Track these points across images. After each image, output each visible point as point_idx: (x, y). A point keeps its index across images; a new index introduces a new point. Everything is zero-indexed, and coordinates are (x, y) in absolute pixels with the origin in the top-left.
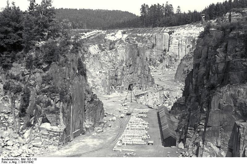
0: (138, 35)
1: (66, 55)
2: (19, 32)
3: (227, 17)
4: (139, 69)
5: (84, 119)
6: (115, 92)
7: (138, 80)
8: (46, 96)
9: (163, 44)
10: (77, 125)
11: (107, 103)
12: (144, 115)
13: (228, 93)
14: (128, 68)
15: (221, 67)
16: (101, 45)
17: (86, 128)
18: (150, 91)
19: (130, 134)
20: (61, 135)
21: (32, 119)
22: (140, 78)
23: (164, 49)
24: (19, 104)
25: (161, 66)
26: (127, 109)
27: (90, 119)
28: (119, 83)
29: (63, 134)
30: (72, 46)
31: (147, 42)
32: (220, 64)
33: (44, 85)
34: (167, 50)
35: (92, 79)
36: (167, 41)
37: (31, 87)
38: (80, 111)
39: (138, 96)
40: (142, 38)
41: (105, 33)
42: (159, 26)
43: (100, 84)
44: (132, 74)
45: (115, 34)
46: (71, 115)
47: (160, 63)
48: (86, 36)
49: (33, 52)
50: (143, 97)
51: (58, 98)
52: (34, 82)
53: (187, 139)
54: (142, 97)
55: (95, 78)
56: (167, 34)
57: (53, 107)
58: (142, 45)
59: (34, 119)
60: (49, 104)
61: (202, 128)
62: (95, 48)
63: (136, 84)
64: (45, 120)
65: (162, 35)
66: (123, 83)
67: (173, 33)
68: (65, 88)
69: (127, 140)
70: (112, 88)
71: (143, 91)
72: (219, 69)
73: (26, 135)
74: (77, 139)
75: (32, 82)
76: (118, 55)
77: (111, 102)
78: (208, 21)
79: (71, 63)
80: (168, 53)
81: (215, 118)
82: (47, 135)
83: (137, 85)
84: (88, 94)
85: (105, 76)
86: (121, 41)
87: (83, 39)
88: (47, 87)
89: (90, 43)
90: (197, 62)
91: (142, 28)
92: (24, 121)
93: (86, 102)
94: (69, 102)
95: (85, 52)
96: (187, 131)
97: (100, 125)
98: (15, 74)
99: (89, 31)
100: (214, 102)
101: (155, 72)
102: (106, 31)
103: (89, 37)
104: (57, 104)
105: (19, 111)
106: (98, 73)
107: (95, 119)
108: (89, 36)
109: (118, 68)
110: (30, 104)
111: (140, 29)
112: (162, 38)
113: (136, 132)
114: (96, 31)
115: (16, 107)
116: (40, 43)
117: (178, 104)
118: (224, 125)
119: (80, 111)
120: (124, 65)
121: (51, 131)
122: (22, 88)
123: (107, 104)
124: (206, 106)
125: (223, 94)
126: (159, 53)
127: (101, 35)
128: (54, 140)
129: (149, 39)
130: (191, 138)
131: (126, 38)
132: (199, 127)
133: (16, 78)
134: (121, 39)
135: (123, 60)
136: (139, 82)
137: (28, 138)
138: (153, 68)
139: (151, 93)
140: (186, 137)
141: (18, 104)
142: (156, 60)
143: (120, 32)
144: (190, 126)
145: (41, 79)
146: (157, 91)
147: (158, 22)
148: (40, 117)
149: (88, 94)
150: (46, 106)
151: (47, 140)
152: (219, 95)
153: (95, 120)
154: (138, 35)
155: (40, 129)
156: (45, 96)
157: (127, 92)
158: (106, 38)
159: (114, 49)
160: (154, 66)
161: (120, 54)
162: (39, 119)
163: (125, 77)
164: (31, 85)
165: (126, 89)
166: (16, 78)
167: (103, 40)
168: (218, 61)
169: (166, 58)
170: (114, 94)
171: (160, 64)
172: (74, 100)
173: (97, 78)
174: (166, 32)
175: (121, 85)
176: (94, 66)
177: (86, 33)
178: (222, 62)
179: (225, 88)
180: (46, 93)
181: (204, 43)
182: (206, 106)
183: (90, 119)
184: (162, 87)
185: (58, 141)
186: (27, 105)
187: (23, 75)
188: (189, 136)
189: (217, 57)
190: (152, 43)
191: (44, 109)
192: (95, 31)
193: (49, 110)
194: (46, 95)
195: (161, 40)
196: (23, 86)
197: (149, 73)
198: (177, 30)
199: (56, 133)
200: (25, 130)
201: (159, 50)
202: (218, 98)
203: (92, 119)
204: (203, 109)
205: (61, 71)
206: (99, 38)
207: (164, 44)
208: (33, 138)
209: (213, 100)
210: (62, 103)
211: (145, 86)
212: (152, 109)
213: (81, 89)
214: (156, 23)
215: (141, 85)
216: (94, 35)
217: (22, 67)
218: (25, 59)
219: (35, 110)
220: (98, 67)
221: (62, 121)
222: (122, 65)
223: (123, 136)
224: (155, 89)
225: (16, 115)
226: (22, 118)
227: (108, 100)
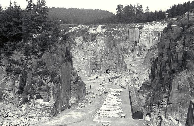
0: (115, 29)
1: (56, 45)
2: (20, 26)
4: (114, 56)
5: (70, 96)
7: (114, 65)
8: (40, 77)
10: (65, 101)
12: (118, 93)
14: (106, 56)
15: (180, 56)
16: (85, 37)
17: (72, 104)
19: (106, 109)
20: (52, 109)
22: (115, 64)
23: (135, 41)
24: (18, 84)
25: (132, 54)
26: (104, 88)
28: (98, 68)
29: (53, 108)
30: (61, 37)
31: (121, 35)
33: (38, 69)
35: (77, 64)
36: (138, 35)
38: (67, 90)
39: (113, 79)
40: (118, 32)
41: (88, 28)
43: (83, 69)
44: (109, 61)
45: (96, 28)
50: (118, 79)
51: (49, 79)
52: (30, 66)
53: (152, 113)
54: (116, 79)
55: (80, 63)
56: (138, 29)
57: (45, 86)
59: (30, 95)
60: (42, 83)
61: (164, 104)
62: (80, 39)
63: (112, 68)
64: (39, 97)
66: (102, 67)
68: (55, 71)
69: (103, 114)
70: (93, 71)
73: (23, 108)
74: (64, 112)
75: (29, 66)
76: (98, 46)
77: (92, 82)
78: (171, 19)
79: (61, 51)
81: (175, 97)
82: (40, 109)
84: (74, 76)
85: (88, 62)
86: (101, 34)
88: (41, 70)
90: (161, 52)
92: (22, 97)
93: (72, 82)
94: (58, 82)
95: (72, 42)
96: (152, 107)
97: (83, 101)
98: (16, 60)
99: (75, 26)
100: (174, 84)
101: (127, 59)
102: (89, 26)
103: (75, 31)
105: (18, 89)
106: (82, 59)
107: (79, 96)
109: (97, 56)
110: (27, 84)
111: (116, 24)
112: (134, 32)
113: (111, 107)
114: (81, 26)
115: (16, 86)
116: (36, 35)
117: (145, 85)
118: (181, 103)
119: (67, 90)
120: (103, 53)
121: (43, 105)
122: (21, 71)
124: (168, 87)
125: (181, 78)
126: (131, 44)
127: (85, 29)
128: (46, 113)
129: (123, 32)
130: (155, 113)
132: (162, 104)
133: (16, 63)
134: (101, 32)
136: (114, 67)
137: (25, 111)
138: (126, 56)
139: (124, 76)
140: (151, 112)
141: (17, 84)
143: (100, 27)
144: (155, 103)
145: (36, 63)
146: (129, 75)
147: (131, 19)
148: (35, 94)
149: (74, 76)
150: (40, 86)
151: (40, 113)
152: (178, 78)
153: (79, 97)
154: (115, 29)
155: (35, 104)
156: (39, 77)
157: (105, 75)
158: (88, 31)
159: (95, 41)
160: (127, 55)
161: (100, 45)
162: (34, 95)
163: (103, 63)
164: (28, 68)
165: (104, 72)
166: (16, 63)
168: (177, 51)
169: (137, 48)
172: (63, 81)
173: (81, 64)
174: (137, 27)
175: (100, 69)
176: (79, 54)
177: (73, 27)
178: (181, 52)
181: (167, 36)
182: (168, 87)
183: (75, 96)
185: (49, 114)
186: (25, 84)
187: (22, 60)
188: (154, 111)
190: (125, 36)
191: (38, 88)
192: (80, 26)
193: (42, 89)
194: (40, 76)
195: (132, 33)
196: (22, 69)
197: (123, 60)
198: (146, 26)
199: (47, 107)
200: (23, 104)
201: (131, 42)
202: (177, 81)
203: (77, 96)
204: (165, 89)
205: (52, 57)
207: (135, 37)
208: (29, 111)
210: (52, 83)
211: (119, 70)
212: (124, 89)
213: (68, 72)
214: (129, 20)
215: (117, 69)
217: (21, 54)
218: (23, 48)
219: (31, 89)
221: (53, 97)
222: (101, 53)
223: (101, 110)
224: (127, 73)
225: (16, 92)
226: (21, 95)
227: (89, 81)
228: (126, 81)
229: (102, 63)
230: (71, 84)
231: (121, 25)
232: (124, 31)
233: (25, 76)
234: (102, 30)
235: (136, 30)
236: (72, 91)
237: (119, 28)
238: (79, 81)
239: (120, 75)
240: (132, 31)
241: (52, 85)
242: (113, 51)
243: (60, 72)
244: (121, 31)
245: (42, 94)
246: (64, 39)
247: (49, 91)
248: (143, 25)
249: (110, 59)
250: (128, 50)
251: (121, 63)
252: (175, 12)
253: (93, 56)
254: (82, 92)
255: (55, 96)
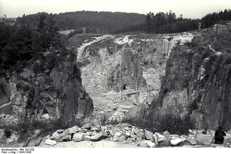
0: (142, 40)
1: (64, 63)
2: (29, 45)
3: (215, 28)
6: (111, 91)
8: (47, 93)
9: (163, 49)
11: (102, 100)
13: (173, 96)
14: (123, 71)
16: (110, 49)
18: (141, 90)
21: (36, 110)
22: (133, 79)
23: (163, 53)
24: (26, 99)
25: (160, 68)
26: (115, 105)
27: (81, 112)
28: (115, 84)
30: (69, 55)
31: (148, 47)
32: (172, 74)
33: (46, 85)
34: (166, 55)
35: (94, 79)
37: (36, 86)
38: (73, 106)
39: (129, 95)
40: (145, 43)
41: (113, 38)
42: (161, 33)
43: (100, 84)
44: (127, 76)
45: (123, 39)
46: (65, 110)
47: (159, 66)
48: (97, 40)
49: (39, 60)
51: (56, 95)
52: (38, 83)
54: (133, 96)
55: (97, 78)
56: (167, 40)
57: (52, 102)
58: (136, 52)
60: (49, 99)
63: (129, 84)
64: (45, 112)
65: (162, 41)
66: (118, 83)
67: (172, 39)
68: (62, 88)
70: (109, 87)
71: (135, 90)
72: (171, 78)
75: (37, 83)
77: (105, 99)
78: (203, 30)
80: (166, 57)
83: (130, 85)
84: (81, 92)
85: (105, 77)
87: (95, 42)
88: (48, 87)
89: (100, 47)
91: (146, 34)
92: (30, 111)
93: (79, 99)
95: (95, 54)
97: (89, 117)
98: (25, 77)
99: (100, 36)
100: (164, 102)
101: (153, 73)
102: (114, 36)
103: (99, 41)
104: (55, 100)
105: (26, 104)
106: (99, 74)
107: (85, 112)
108: (99, 40)
109: (114, 71)
110: (34, 100)
112: (162, 43)
114: (106, 36)
115: (24, 101)
116: (45, 53)
117: (154, 103)
119: (73, 106)
120: (120, 68)
123: (97, 100)
125: (170, 97)
126: (159, 57)
129: (151, 44)
131: (132, 43)
133: (26, 80)
134: (127, 43)
135: (120, 64)
138: (153, 70)
139: (142, 92)
141: (26, 99)
142: (156, 63)
143: (127, 37)
145: (44, 80)
146: (148, 91)
147: (161, 29)
148: (42, 109)
149: (81, 92)
150: (47, 101)
154: (142, 40)
156: (46, 93)
158: (114, 42)
160: (155, 68)
161: (117, 59)
162: (41, 110)
163: (120, 79)
164: (36, 85)
166: (26, 80)
167: (112, 44)
168: (171, 72)
169: (165, 62)
170: (110, 92)
171: (159, 66)
172: (68, 97)
173: (98, 79)
174: (166, 39)
177: (98, 37)
178: (174, 73)
179: (171, 92)
180: (47, 92)
181: (174, 55)
183: (81, 112)
184: (153, 87)
186: (33, 100)
187: (31, 77)
189: (172, 69)
191: (45, 103)
192: (105, 36)
193: (49, 104)
194: (47, 93)
196: (30, 86)
197: (141, 76)
198: (176, 37)
201: (159, 55)
202: (166, 99)
205: (58, 75)
206: (108, 42)
209: (164, 101)
210: (58, 99)
211: (137, 86)
212: (136, 106)
213: (75, 89)
214: (159, 30)
215: (134, 85)
216: (104, 40)
218: (32, 66)
220: (100, 69)
222: (118, 68)
224: (146, 89)
225: (24, 107)
226: (28, 110)
227: (103, 98)
228: (144, 98)
229: (119, 79)
230: (78, 100)
231: (149, 35)
232: (152, 42)
233: (34, 92)
234: (129, 41)
235: (165, 41)
236: (79, 107)
237: (147, 39)
238: (86, 97)
239: (137, 91)
240: (161, 42)
241: (58, 101)
242: (131, 66)
243: (66, 89)
244: (149, 43)
245: (49, 109)
246: (71, 57)
247: (55, 107)
248: (173, 36)
249: (127, 75)
250: (155, 63)
251: (140, 79)
252: (209, 22)
253: (110, 71)
254: (88, 108)
255: (60, 111)
